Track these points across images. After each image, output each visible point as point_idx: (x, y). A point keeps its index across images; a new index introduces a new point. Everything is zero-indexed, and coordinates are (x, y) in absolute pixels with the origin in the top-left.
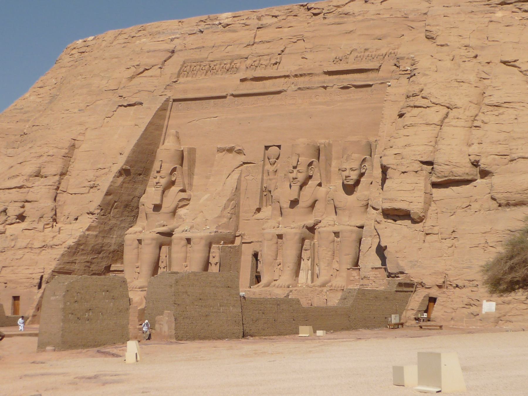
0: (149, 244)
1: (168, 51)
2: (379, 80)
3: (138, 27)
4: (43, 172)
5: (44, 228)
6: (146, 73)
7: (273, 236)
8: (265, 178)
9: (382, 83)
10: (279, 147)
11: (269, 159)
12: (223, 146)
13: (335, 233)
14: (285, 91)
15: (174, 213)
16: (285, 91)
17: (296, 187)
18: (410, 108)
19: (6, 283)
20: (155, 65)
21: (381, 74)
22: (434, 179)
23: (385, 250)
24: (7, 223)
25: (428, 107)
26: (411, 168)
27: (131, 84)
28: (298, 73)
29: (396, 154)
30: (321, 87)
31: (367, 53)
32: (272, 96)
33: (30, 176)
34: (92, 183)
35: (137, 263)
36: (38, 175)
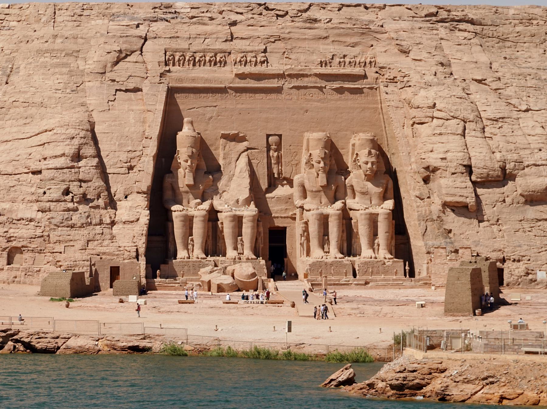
1: (141, 37)
10: (280, 136)
20: (135, 51)
22: (474, 178)
25: (447, 120)
26: (458, 170)
27: (116, 68)
29: (442, 159)
31: (347, 60)
34: (129, 164)
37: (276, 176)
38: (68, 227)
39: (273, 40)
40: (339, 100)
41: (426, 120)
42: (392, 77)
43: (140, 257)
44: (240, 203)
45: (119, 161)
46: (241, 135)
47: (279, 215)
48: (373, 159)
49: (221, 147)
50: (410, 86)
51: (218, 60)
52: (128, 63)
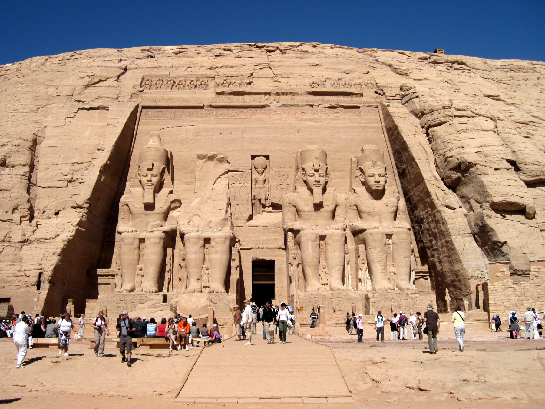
1: (120, 68)
2: (365, 104)
5: (21, 221)
6: (101, 84)
7: (317, 237)
8: (253, 186)
10: (267, 157)
11: (256, 169)
12: (204, 153)
13: (387, 235)
14: (269, 106)
16: (269, 106)
17: (317, 191)
18: (451, 118)
20: (110, 78)
21: (364, 99)
23: (502, 246)
28: (280, 91)
29: (476, 152)
30: (306, 105)
32: (254, 110)
34: (70, 177)
35: (138, 264)
37: (263, 202)
39: (261, 67)
40: (335, 119)
41: (446, 119)
43: (42, 285)
44: (213, 225)
45: (59, 174)
46: (220, 156)
47: (265, 246)
48: (382, 172)
49: (197, 169)
50: (417, 97)
52: (100, 88)
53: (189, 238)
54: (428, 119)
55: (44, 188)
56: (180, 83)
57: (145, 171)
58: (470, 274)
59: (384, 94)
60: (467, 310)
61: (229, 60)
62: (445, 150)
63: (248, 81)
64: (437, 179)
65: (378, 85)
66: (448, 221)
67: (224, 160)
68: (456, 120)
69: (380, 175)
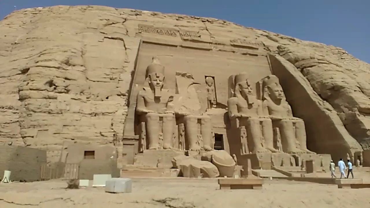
0: (171, 120)
3: (87, 6)
4: (71, 62)
6: (113, 25)
9: (263, 55)
10: (213, 78)
11: (207, 83)
12: (180, 72)
14: (212, 50)
15: (167, 104)
16: (212, 50)
18: (318, 64)
19: (73, 139)
23: (367, 131)
24: (56, 91)
25: (329, 64)
28: (218, 43)
29: (342, 81)
33: (62, 62)
34: (111, 76)
36: (67, 63)
38: (45, 112)
39: (203, 29)
40: (245, 60)
41: (315, 64)
42: (275, 50)
46: (188, 75)
50: (290, 52)
51: (171, 33)
53: (190, 118)
54: (303, 63)
55: (94, 81)
56: (161, 32)
57: (155, 78)
58: (351, 146)
59: (269, 50)
60: (359, 166)
61: (184, 22)
62: (322, 79)
63: (199, 35)
64: (316, 95)
65: (265, 45)
66: (331, 117)
67: (190, 76)
68: (321, 65)
69: (281, 91)
